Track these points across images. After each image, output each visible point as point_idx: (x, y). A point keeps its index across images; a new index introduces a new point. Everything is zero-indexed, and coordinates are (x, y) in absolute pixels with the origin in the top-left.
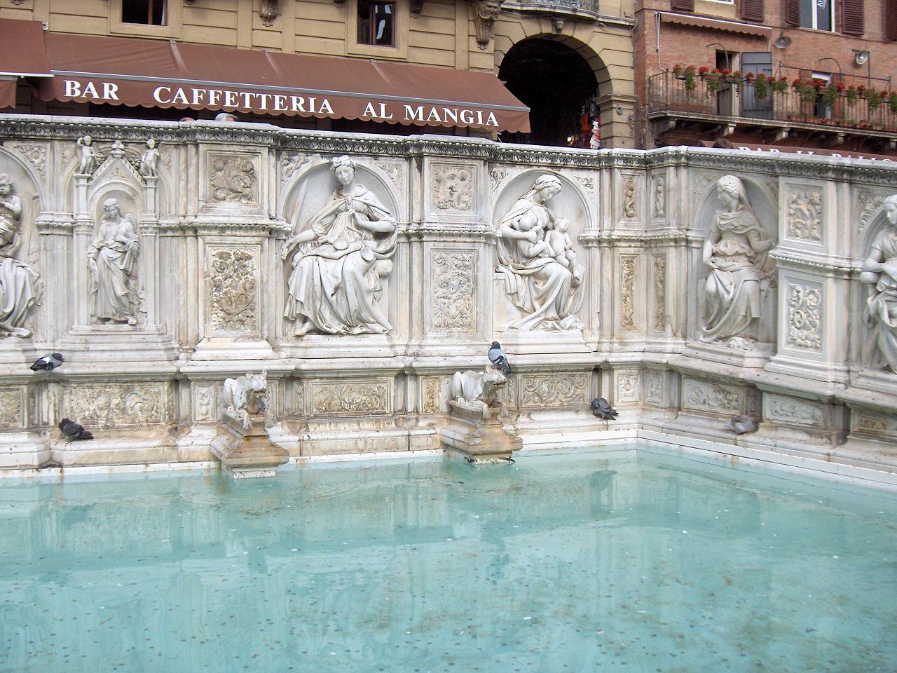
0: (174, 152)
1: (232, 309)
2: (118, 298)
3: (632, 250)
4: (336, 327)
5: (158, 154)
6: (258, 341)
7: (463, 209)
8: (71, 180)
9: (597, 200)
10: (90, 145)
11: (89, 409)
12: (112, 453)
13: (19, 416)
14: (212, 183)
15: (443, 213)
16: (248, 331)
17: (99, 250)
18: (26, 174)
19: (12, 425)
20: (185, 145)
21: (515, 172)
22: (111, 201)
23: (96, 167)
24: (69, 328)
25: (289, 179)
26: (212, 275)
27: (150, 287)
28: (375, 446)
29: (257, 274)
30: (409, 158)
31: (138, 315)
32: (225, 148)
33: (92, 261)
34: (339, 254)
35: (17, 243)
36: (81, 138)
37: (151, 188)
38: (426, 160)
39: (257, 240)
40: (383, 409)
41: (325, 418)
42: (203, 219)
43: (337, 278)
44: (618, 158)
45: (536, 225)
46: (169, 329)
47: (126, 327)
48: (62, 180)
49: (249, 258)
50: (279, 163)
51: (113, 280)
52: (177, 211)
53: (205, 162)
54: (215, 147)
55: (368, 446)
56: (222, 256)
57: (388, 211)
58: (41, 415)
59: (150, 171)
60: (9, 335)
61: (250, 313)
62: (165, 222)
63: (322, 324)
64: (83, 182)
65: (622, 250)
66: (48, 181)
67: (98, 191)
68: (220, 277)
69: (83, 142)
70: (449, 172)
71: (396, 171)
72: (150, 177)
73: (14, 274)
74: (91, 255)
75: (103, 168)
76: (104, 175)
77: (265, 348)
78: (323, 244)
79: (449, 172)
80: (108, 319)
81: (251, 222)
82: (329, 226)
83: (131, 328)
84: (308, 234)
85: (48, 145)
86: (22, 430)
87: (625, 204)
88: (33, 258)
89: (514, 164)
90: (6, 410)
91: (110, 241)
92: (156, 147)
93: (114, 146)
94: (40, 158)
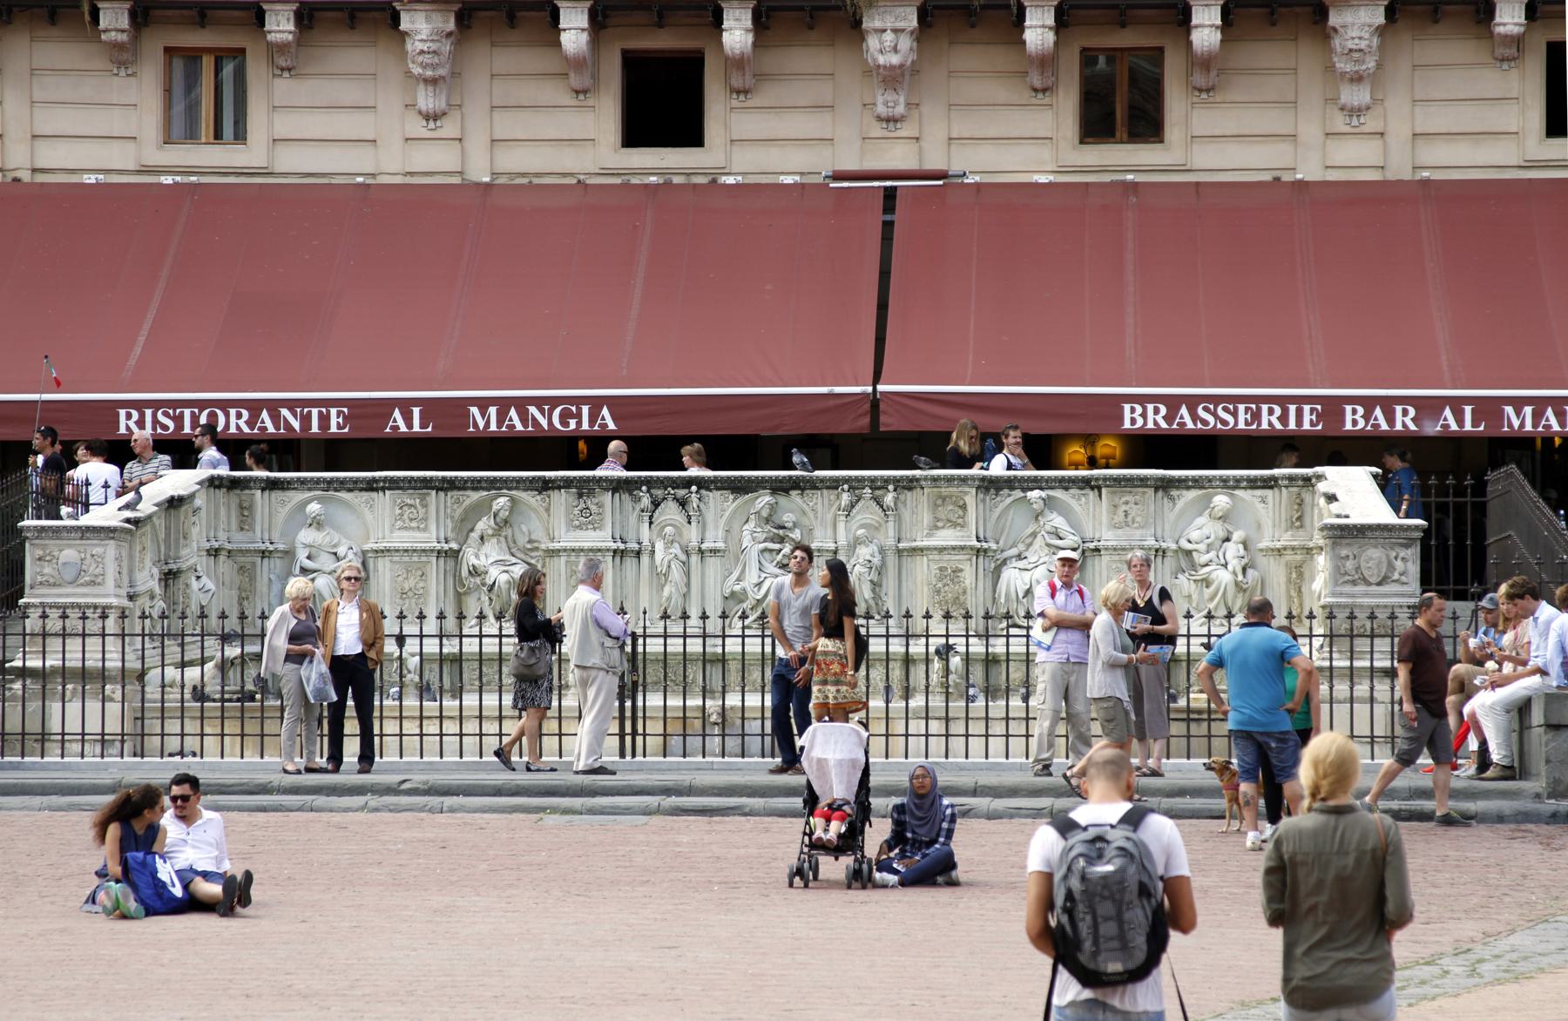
0: (909, 494)
2: (866, 601)
3: (1299, 557)
7: (1136, 528)
9: (1271, 514)
15: (1120, 532)
18: (804, 513)
20: (915, 487)
21: (1193, 494)
22: (861, 532)
23: (853, 507)
26: (934, 583)
27: (891, 593)
29: (967, 582)
30: (1092, 488)
32: (943, 490)
38: (1104, 491)
39: (967, 557)
42: (926, 543)
44: (1282, 478)
45: (1208, 538)
48: (830, 516)
49: (961, 570)
50: (988, 498)
53: (928, 501)
54: (935, 490)
56: (941, 569)
62: (901, 545)
64: (843, 518)
65: (1288, 558)
67: (854, 524)
68: (940, 585)
69: (843, 490)
70: (1124, 499)
72: (890, 512)
75: (857, 508)
76: (858, 513)
79: (1124, 499)
81: (962, 543)
84: (1014, 551)
85: (819, 492)
87: (1292, 517)
89: (1188, 488)
91: (861, 560)
92: (895, 490)
93: (865, 491)
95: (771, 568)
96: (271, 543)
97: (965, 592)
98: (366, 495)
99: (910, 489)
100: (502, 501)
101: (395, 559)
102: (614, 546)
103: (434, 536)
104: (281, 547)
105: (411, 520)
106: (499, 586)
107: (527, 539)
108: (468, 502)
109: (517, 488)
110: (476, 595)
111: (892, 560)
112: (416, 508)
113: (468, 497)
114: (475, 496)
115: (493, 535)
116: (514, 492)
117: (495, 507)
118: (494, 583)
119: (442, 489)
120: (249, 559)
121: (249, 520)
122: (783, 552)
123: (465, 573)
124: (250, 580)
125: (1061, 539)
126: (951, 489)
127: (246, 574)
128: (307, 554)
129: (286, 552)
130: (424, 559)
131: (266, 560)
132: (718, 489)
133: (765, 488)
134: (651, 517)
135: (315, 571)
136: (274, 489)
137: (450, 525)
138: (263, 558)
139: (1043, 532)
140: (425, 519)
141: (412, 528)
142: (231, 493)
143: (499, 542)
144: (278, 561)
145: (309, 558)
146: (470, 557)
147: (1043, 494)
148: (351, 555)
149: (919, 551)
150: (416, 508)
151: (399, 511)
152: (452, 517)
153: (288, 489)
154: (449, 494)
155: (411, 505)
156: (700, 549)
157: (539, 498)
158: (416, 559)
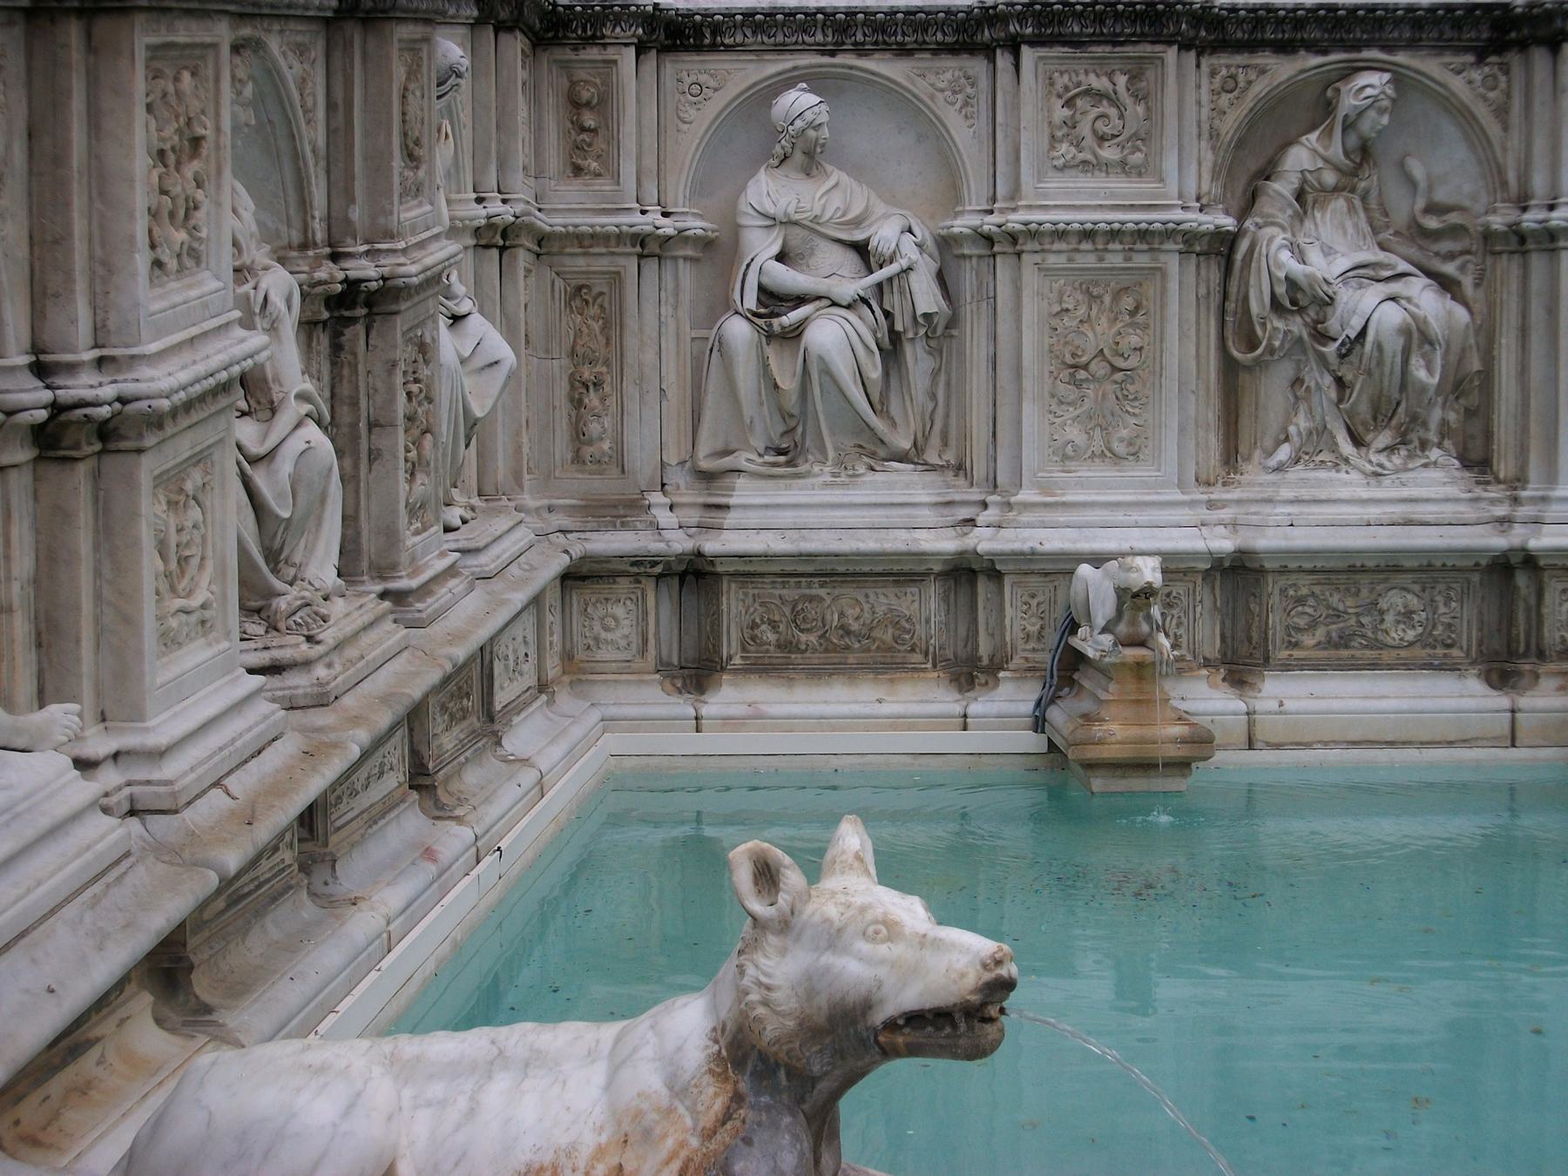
96: (665, 215)
98: (951, 68)
100: (1374, 82)
101: (1052, 260)
103: (1173, 188)
104: (696, 226)
105: (1102, 139)
106: (1379, 346)
107: (1420, 204)
108: (1260, 87)
109: (1412, 45)
110: (1282, 373)
112: (1114, 101)
113: (1263, 72)
114: (1282, 70)
115: (1336, 189)
116: (1401, 58)
117: (1349, 101)
118: (1363, 333)
120: (603, 264)
121: (600, 144)
123: (1258, 305)
124: (605, 328)
127: (594, 310)
128: (775, 249)
129: (707, 244)
130: (1142, 260)
131: (651, 266)
135: (800, 300)
136: (664, 50)
138: (641, 256)
140: (1141, 139)
141: (1105, 167)
142: (544, 58)
143: (1351, 209)
144: (685, 271)
145: (781, 257)
148: (910, 252)
150: (1114, 101)
152: (1214, 135)
153: (714, 48)
154: (1205, 62)
155: (1097, 96)
157: (1476, 75)
158: (1115, 260)
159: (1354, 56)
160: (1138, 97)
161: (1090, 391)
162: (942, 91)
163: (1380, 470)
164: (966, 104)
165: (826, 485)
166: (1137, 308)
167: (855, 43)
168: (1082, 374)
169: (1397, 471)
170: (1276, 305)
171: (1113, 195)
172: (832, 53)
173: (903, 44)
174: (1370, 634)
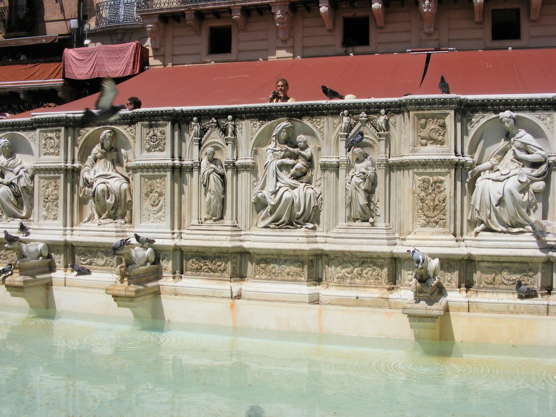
1: (430, 214)
4: (500, 228)
5: (387, 118)
6: (447, 235)
8: (338, 137)
10: (348, 116)
11: (341, 273)
12: (350, 299)
13: (303, 274)
14: (418, 134)
16: (441, 229)
17: (352, 177)
19: (299, 278)
24: (336, 224)
25: (472, 129)
26: (419, 192)
28: (522, 310)
31: (375, 217)
32: (426, 112)
33: (348, 184)
34: (504, 177)
35: (309, 175)
36: (342, 112)
37: (383, 140)
39: (447, 170)
40: (533, 285)
41: (490, 288)
43: (500, 194)
46: (394, 227)
47: (367, 224)
48: (333, 137)
50: (465, 119)
51: (358, 196)
52: (400, 153)
54: (420, 112)
55: (517, 309)
57: (540, 147)
58: (317, 273)
59: (382, 130)
60: (301, 227)
61: (442, 217)
62: (391, 160)
63: (491, 225)
66: (325, 138)
71: (548, 119)
72: (382, 132)
73: (304, 192)
74: (348, 181)
77: (450, 240)
78: (496, 171)
80: (358, 219)
82: (500, 160)
83: (369, 225)
86: (304, 281)
88: (318, 183)
90: (296, 269)
91: (357, 173)
92: (386, 114)
93: (361, 115)
94: (321, 125)
95: (286, 177)
97: (444, 201)
99: (398, 113)
102: (170, 162)
105: (52, 147)
106: (97, 194)
111: (381, 174)
119: (70, 126)
122: (296, 166)
125: (528, 153)
126: (433, 112)
130: (57, 175)
132: (248, 118)
133: (283, 116)
134: (200, 141)
137: (77, 150)
139: (513, 148)
140: (58, 147)
146: (87, 174)
147: (514, 114)
149: (403, 166)
151: (44, 142)
155: (51, 138)
156: (234, 163)
157: (128, 130)
159: (105, 126)
160: (58, 138)
161: (48, 204)
162: (31, 138)
163: (100, 223)
164: (35, 141)
165: (3, 223)
166: (56, 185)
167: (16, 129)
168: (46, 200)
169: (104, 224)
170: (85, 185)
171: (52, 160)
172: (13, 131)
173: (17, 128)
174: (95, 262)
